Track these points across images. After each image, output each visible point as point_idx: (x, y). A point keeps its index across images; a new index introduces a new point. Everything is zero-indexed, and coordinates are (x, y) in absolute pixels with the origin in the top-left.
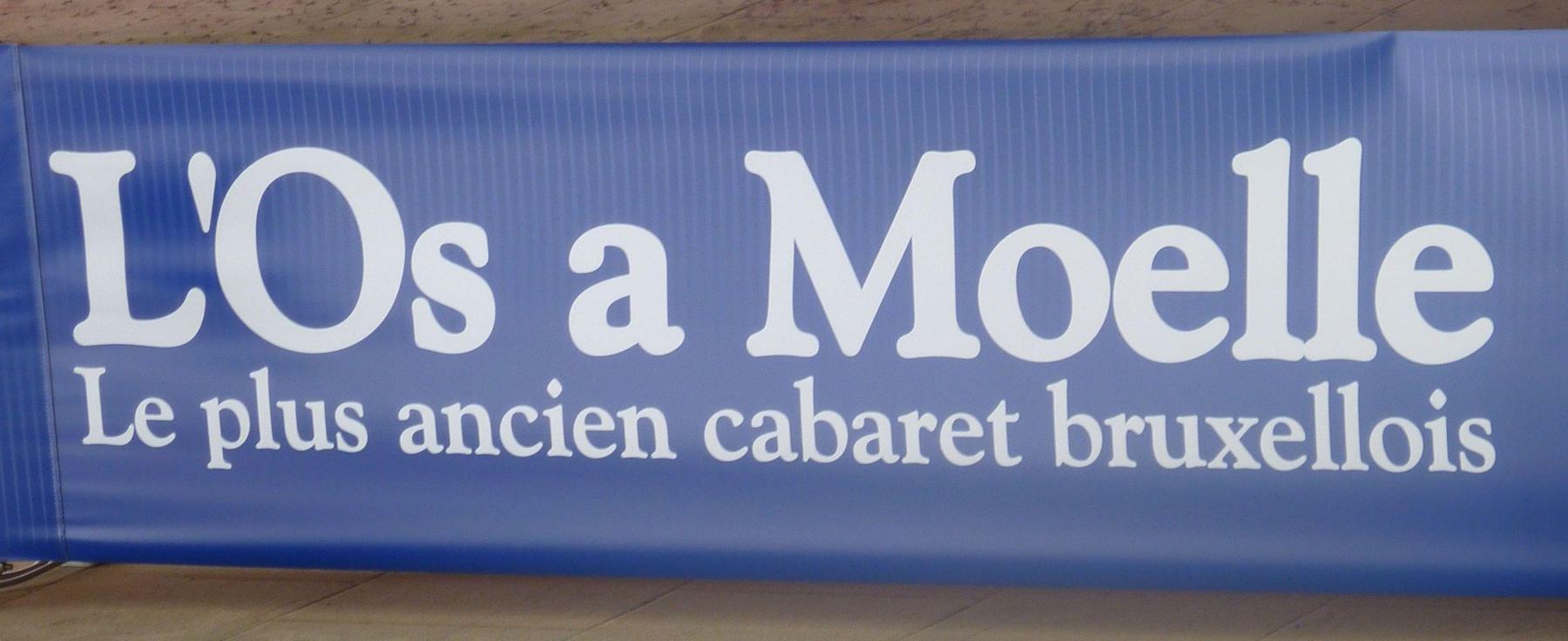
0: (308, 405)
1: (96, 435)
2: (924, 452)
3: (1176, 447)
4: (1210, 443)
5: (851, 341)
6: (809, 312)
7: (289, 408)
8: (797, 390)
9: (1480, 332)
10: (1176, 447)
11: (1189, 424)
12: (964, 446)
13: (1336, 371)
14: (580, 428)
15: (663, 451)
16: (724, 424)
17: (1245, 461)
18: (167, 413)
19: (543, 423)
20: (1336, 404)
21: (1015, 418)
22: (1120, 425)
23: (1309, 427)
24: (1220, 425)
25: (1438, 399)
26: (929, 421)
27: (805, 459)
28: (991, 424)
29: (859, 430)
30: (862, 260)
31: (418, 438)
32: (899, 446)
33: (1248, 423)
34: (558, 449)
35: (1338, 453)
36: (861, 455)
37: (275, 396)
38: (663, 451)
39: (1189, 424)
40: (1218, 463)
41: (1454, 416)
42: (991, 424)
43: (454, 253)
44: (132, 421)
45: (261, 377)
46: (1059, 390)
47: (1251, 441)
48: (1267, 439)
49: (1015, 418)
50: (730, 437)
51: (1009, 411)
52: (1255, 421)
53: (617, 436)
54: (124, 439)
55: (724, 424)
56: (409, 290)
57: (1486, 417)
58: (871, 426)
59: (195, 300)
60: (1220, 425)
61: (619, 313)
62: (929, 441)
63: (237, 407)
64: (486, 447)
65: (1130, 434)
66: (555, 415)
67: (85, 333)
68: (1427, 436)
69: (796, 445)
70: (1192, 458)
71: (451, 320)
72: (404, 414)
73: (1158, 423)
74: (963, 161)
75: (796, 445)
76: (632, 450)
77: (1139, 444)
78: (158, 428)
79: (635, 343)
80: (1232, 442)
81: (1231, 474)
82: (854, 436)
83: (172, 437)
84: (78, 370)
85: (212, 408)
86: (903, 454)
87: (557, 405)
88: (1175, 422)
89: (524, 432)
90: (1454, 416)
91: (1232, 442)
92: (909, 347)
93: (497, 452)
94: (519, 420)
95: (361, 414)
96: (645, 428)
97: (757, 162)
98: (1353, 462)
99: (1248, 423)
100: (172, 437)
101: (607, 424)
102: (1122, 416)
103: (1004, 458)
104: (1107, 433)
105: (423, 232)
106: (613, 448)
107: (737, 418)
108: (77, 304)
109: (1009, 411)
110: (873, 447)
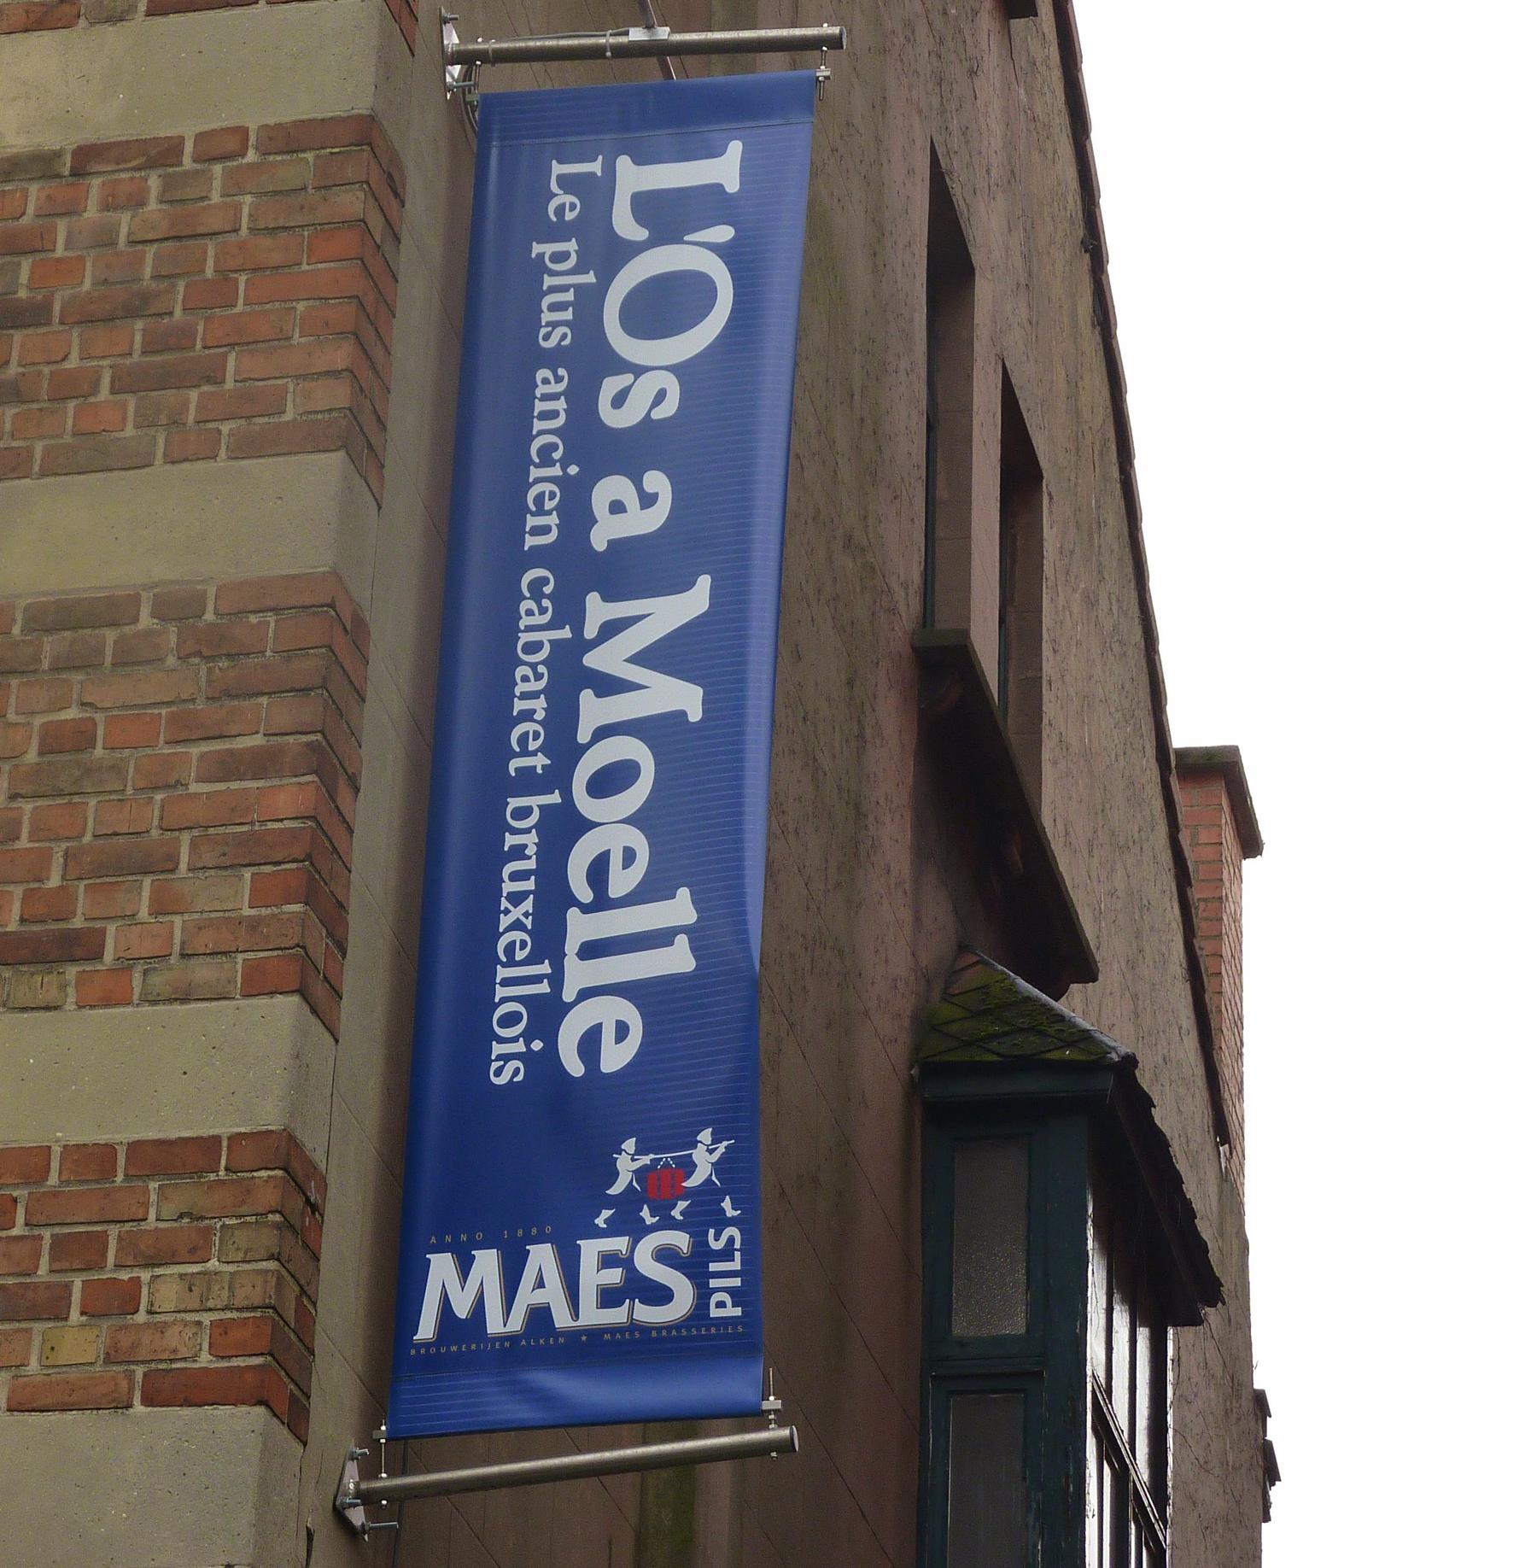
0: (571, 309)
1: (558, 169)
2: (521, 712)
3: (515, 876)
4: (517, 898)
5: (592, 660)
6: (611, 629)
7: (569, 296)
8: (588, 273)
9: (574, 1067)
10: (515, 876)
11: (530, 885)
12: (523, 739)
13: (557, 979)
14: (547, 487)
15: (530, 541)
16: (546, 581)
17: (505, 922)
18: (570, 216)
19: (552, 463)
20: (536, 979)
21: (539, 771)
22: (531, 840)
23: (526, 962)
24: (528, 905)
25: (537, 1045)
26: (540, 716)
27: (520, 634)
28: (536, 755)
29: (557, 372)
30: (638, 659)
31: (546, 381)
32: (525, 696)
33: (528, 923)
34: (535, 473)
35: (507, 982)
36: (520, 671)
37: (578, 288)
38: (530, 541)
39: (530, 885)
40: (504, 904)
41: (526, 1057)
42: (536, 755)
43: (661, 396)
44: (566, 193)
45: (590, 278)
46: (555, 798)
47: (517, 925)
48: (518, 936)
49: (539, 771)
50: (537, 586)
51: (543, 767)
52: (529, 927)
53: (541, 511)
54: (554, 187)
55: (546, 581)
56: (639, 371)
57: (571, 343)
58: (538, 677)
59: (642, 234)
60: (528, 905)
61: (617, 507)
62: (527, 715)
63: (571, 263)
64: (538, 425)
65: (525, 846)
66: (556, 471)
67: (624, 163)
68: (515, 1040)
69: (529, 629)
70: (508, 887)
71: (619, 400)
72: (562, 372)
73: (531, 864)
74: (695, 714)
75: (529, 629)
76: (531, 521)
77: (519, 852)
78: (560, 210)
79: (598, 519)
80: (517, 913)
81: (497, 912)
82: (533, 666)
83: (555, 219)
84: (600, 157)
85: (571, 246)
86: (521, 698)
87: (526, 1047)
88: (569, 306)
89: (547, 451)
90: (526, 1057)
91: (517, 913)
92: (587, 696)
93: (534, 433)
94: (555, 447)
95: (563, 343)
96: (545, 530)
97: (704, 582)
98: (501, 992)
99: (528, 923)
100: (555, 219)
101: (549, 505)
102: (546, 706)
103: (514, 764)
104: (527, 831)
105: (635, 1005)
106: (533, 509)
107: (548, 590)
108: (641, 158)
109: (543, 767)
110: (525, 679)
